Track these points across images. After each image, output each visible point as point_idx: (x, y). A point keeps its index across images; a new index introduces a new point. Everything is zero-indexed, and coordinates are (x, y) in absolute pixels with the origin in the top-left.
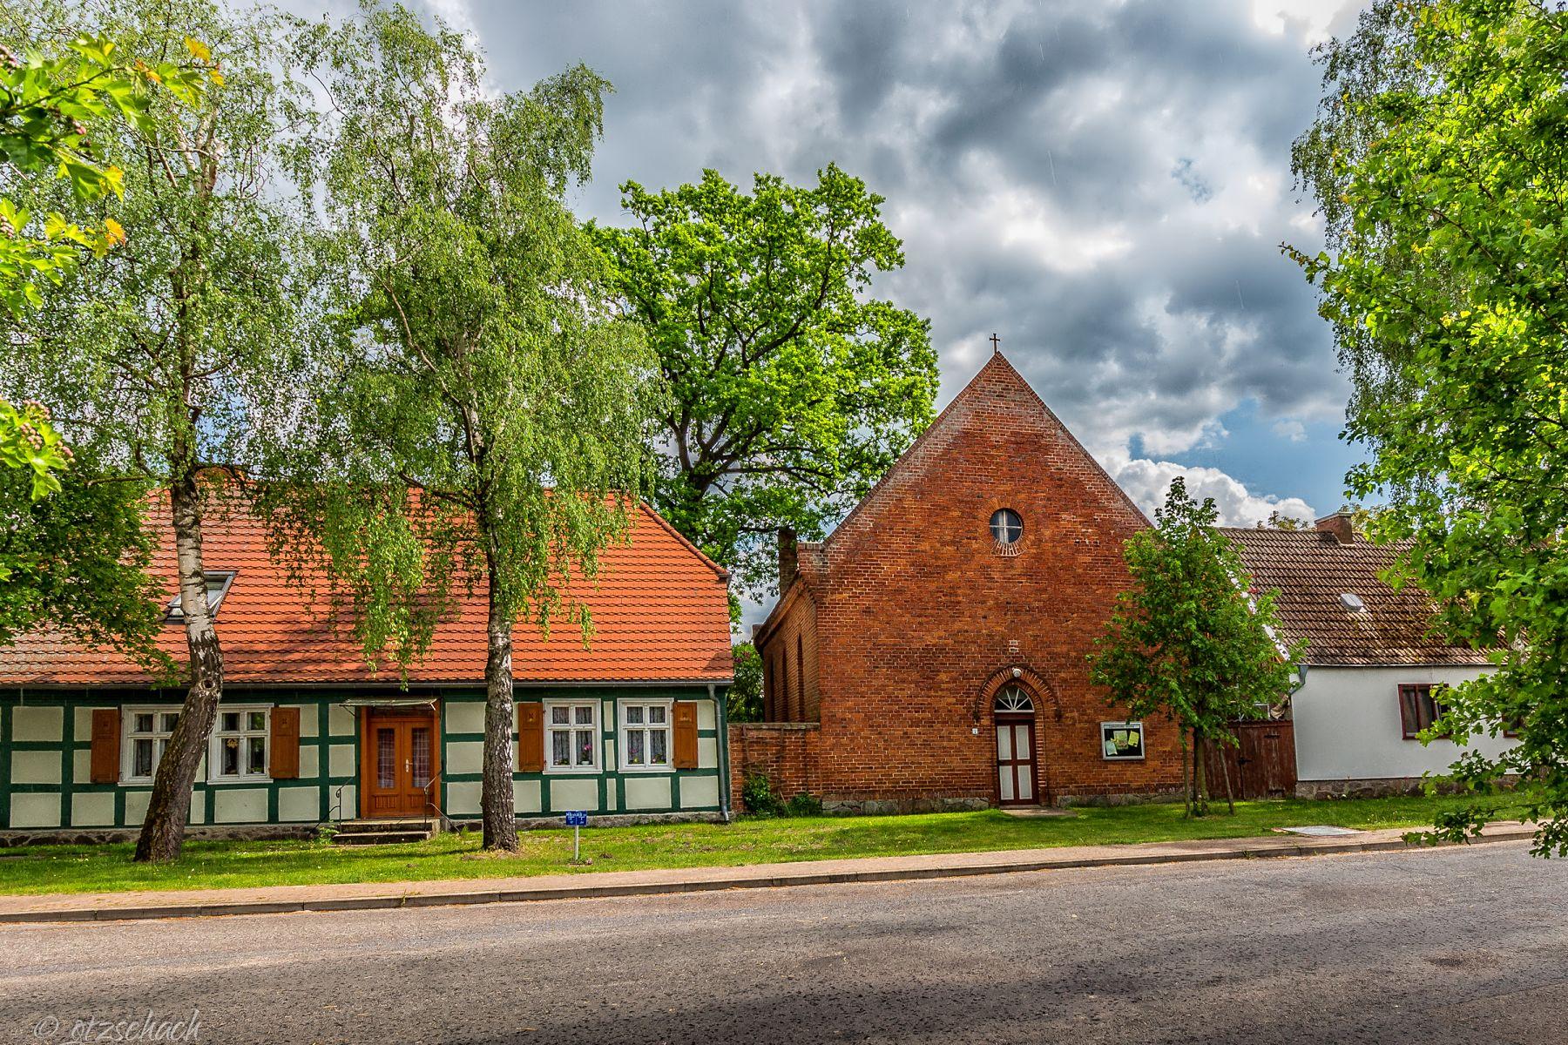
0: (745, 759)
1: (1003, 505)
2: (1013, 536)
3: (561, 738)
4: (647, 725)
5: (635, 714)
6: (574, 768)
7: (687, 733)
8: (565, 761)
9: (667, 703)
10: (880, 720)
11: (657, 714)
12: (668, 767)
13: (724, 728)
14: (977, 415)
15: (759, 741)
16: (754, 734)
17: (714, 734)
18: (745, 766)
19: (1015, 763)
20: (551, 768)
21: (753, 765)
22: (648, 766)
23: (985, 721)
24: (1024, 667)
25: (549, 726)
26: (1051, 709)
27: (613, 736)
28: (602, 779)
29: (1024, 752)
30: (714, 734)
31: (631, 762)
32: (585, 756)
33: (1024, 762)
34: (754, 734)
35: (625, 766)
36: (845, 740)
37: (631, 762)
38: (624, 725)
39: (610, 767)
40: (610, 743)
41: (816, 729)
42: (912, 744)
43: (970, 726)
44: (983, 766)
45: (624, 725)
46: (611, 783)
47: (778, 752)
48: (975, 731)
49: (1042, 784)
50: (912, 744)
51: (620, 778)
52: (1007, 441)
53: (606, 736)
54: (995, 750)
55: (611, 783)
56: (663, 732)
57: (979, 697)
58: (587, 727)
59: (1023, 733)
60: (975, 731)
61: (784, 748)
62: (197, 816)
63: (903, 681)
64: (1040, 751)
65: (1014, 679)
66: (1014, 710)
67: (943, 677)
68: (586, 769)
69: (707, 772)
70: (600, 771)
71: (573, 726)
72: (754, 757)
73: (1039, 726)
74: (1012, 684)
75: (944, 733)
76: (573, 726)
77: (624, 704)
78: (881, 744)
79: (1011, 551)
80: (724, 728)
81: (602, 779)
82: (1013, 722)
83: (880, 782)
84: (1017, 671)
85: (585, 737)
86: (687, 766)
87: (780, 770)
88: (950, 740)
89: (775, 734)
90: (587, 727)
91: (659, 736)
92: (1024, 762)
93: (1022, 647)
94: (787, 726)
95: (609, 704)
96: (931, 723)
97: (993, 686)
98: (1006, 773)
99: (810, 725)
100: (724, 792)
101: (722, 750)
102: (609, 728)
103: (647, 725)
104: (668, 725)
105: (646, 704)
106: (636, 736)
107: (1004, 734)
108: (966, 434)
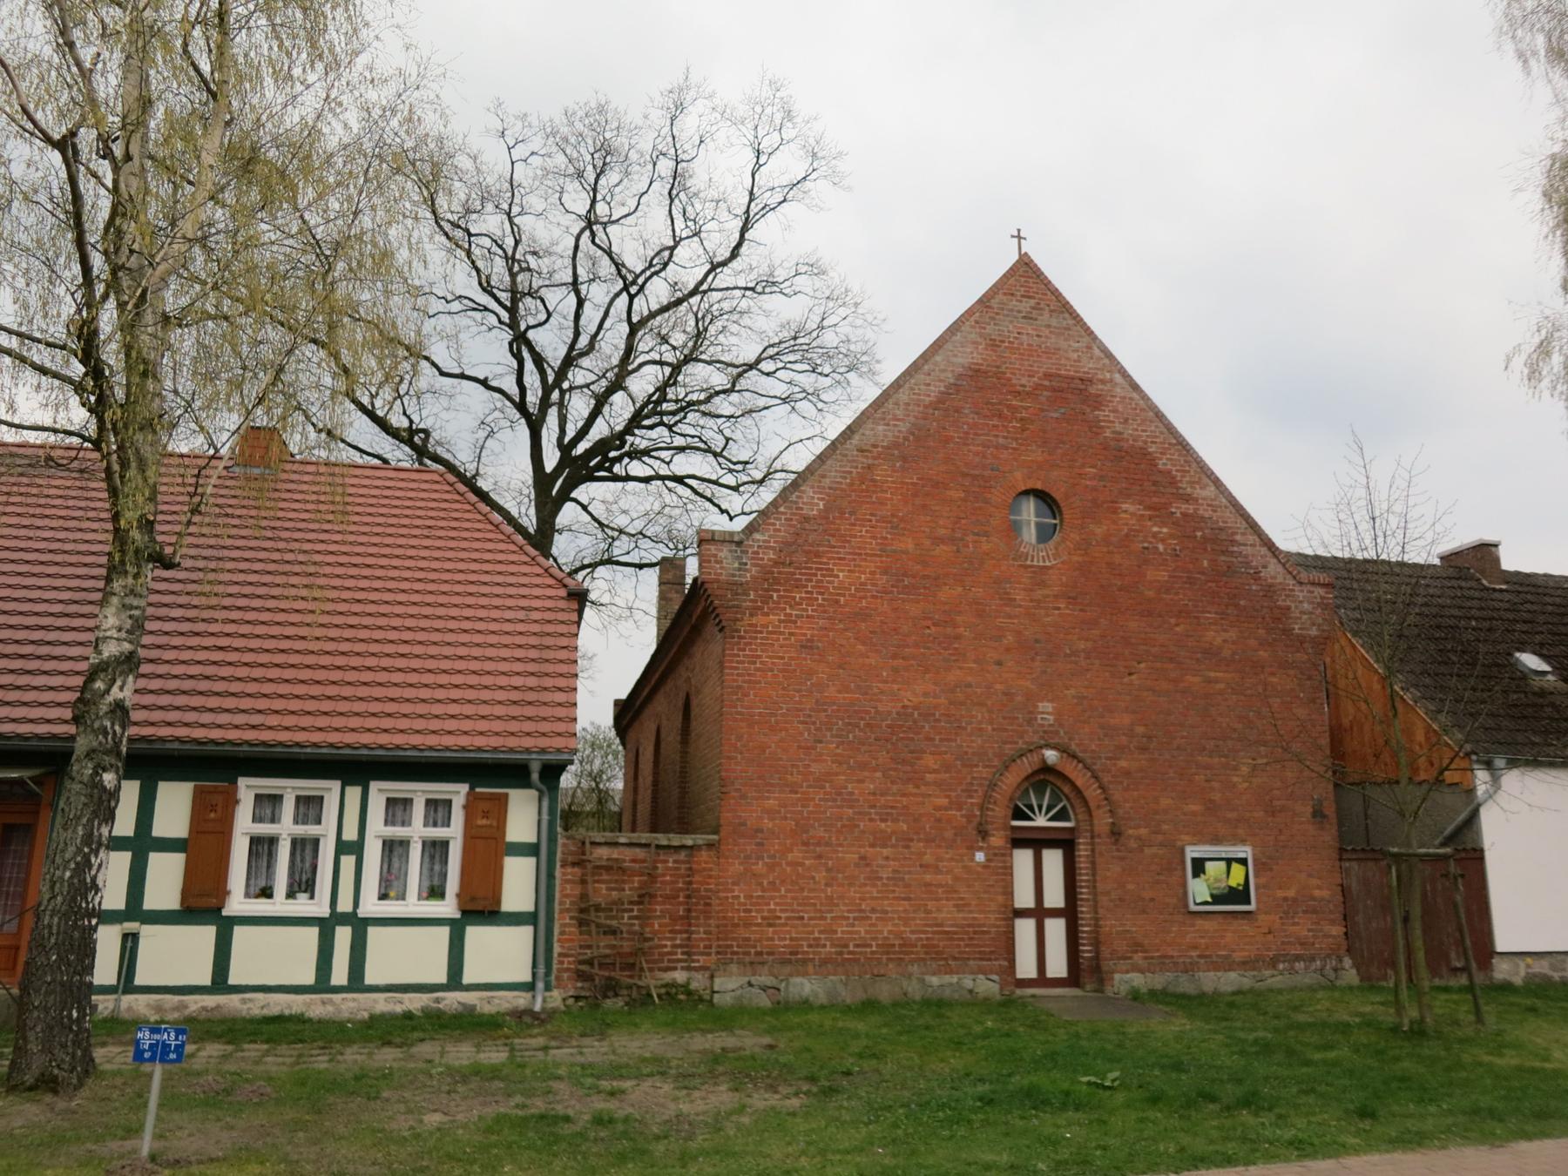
0: (584, 897)
1: (1030, 485)
2: (1045, 534)
3: (262, 848)
4: (417, 830)
5: (397, 809)
6: (279, 905)
7: (487, 849)
8: (267, 893)
9: (458, 793)
10: (821, 833)
11: (438, 810)
12: (447, 908)
13: (552, 839)
14: (993, 344)
15: (612, 867)
16: (603, 853)
17: (531, 850)
18: (585, 914)
19: (1040, 913)
20: (238, 903)
21: (598, 908)
22: (413, 905)
23: (998, 840)
24: (1062, 749)
25: (244, 825)
26: (1103, 821)
27: (355, 848)
28: (326, 928)
29: (1055, 896)
30: (531, 850)
31: (383, 896)
32: (302, 884)
33: (1054, 913)
34: (603, 853)
35: (371, 906)
36: (760, 867)
37: (383, 896)
38: (377, 827)
39: (345, 905)
40: (348, 862)
41: (710, 846)
42: (874, 878)
43: (973, 849)
44: (991, 919)
45: (377, 827)
46: (343, 935)
47: (643, 885)
48: (980, 857)
49: (1086, 950)
50: (874, 878)
51: (361, 926)
52: (1037, 387)
53: (342, 848)
54: (1009, 892)
55: (343, 935)
56: (444, 844)
57: (987, 797)
58: (311, 830)
59: (1053, 860)
60: (980, 857)
61: (652, 877)
62: (105, 970)
63: (863, 766)
64: (1084, 893)
65: (1046, 769)
66: (1041, 821)
67: (929, 761)
68: (302, 906)
69: (516, 919)
70: (324, 911)
71: (286, 827)
72: (602, 892)
73: (1082, 851)
74: (1044, 776)
75: (928, 858)
76: (286, 827)
77: (379, 792)
78: (820, 876)
79: (1042, 556)
80: (552, 839)
81: (326, 928)
82: (1037, 842)
83: (817, 943)
84: (1051, 755)
85: (305, 848)
86: (481, 907)
87: (644, 918)
88: (937, 870)
89: (639, 853)
90: (311, 830)
91: (436, 850)
92: (1054, 913)
93: (1058, 714)
94: (662, 839)
95: (354, 793)
96: (906, 841)
97: (1012, 779)
98: (1025, 930)
99: (700, 839)
100: (542, 955)
101: (545, 884)
102: (350, 834)
103: (417, 830)
104: (454, 832)
105: (420, 792)
106: (393, 848)
107: (1023, 860)
108: (975, 373)
